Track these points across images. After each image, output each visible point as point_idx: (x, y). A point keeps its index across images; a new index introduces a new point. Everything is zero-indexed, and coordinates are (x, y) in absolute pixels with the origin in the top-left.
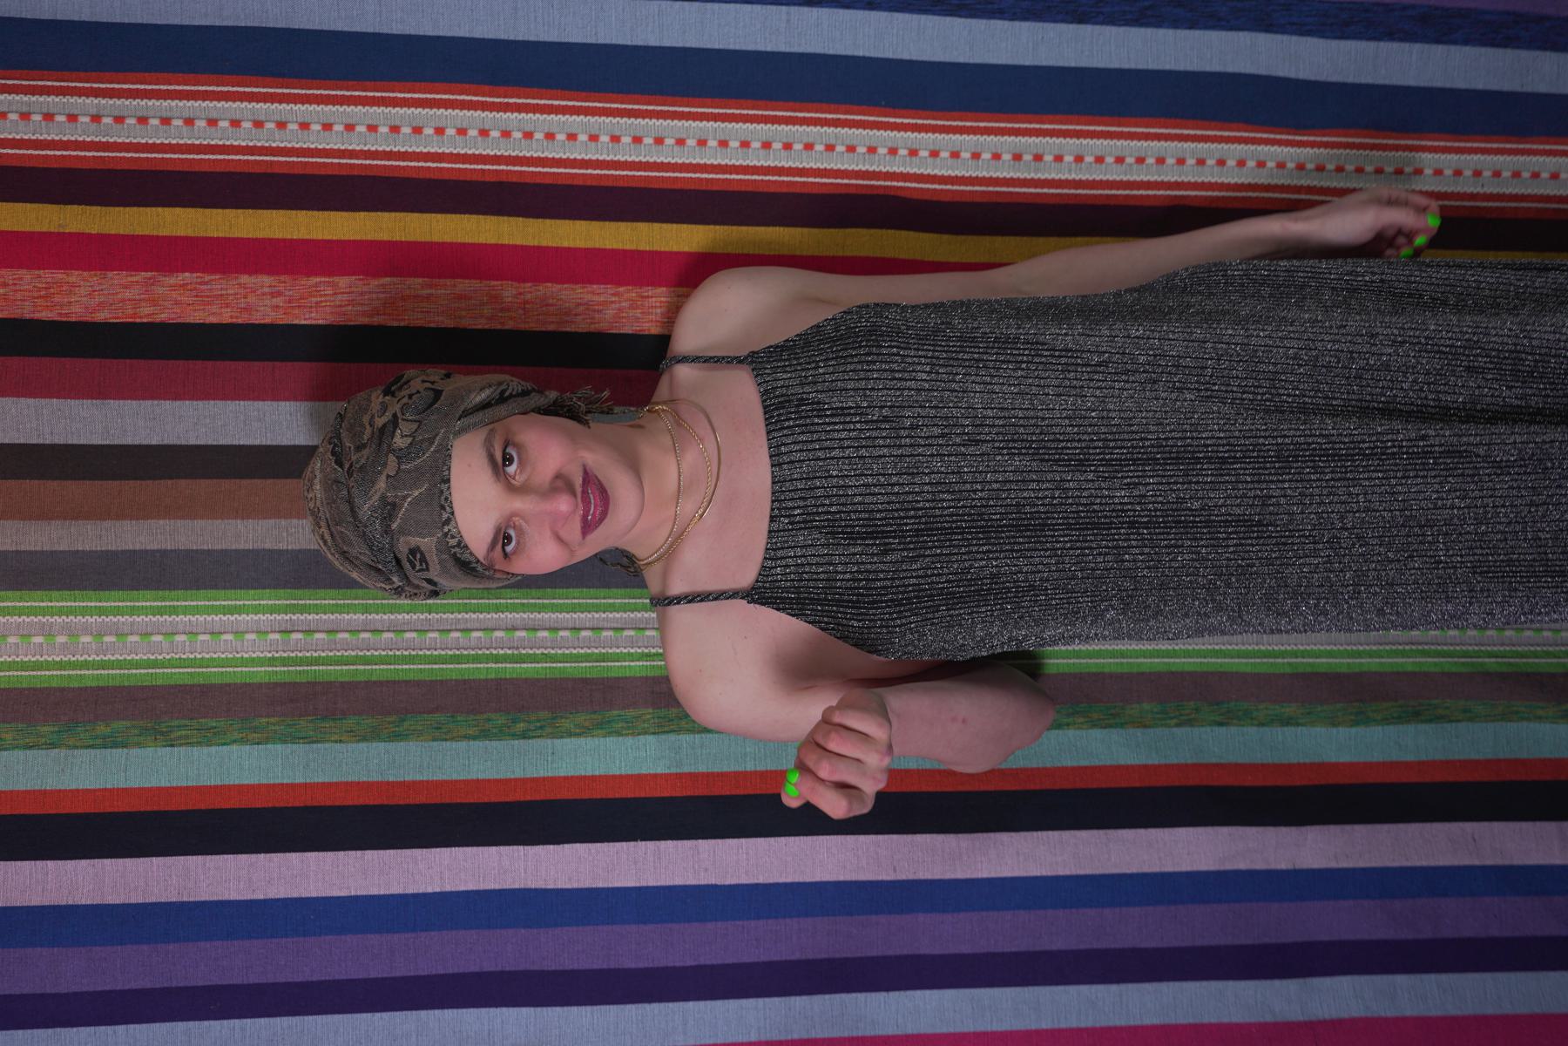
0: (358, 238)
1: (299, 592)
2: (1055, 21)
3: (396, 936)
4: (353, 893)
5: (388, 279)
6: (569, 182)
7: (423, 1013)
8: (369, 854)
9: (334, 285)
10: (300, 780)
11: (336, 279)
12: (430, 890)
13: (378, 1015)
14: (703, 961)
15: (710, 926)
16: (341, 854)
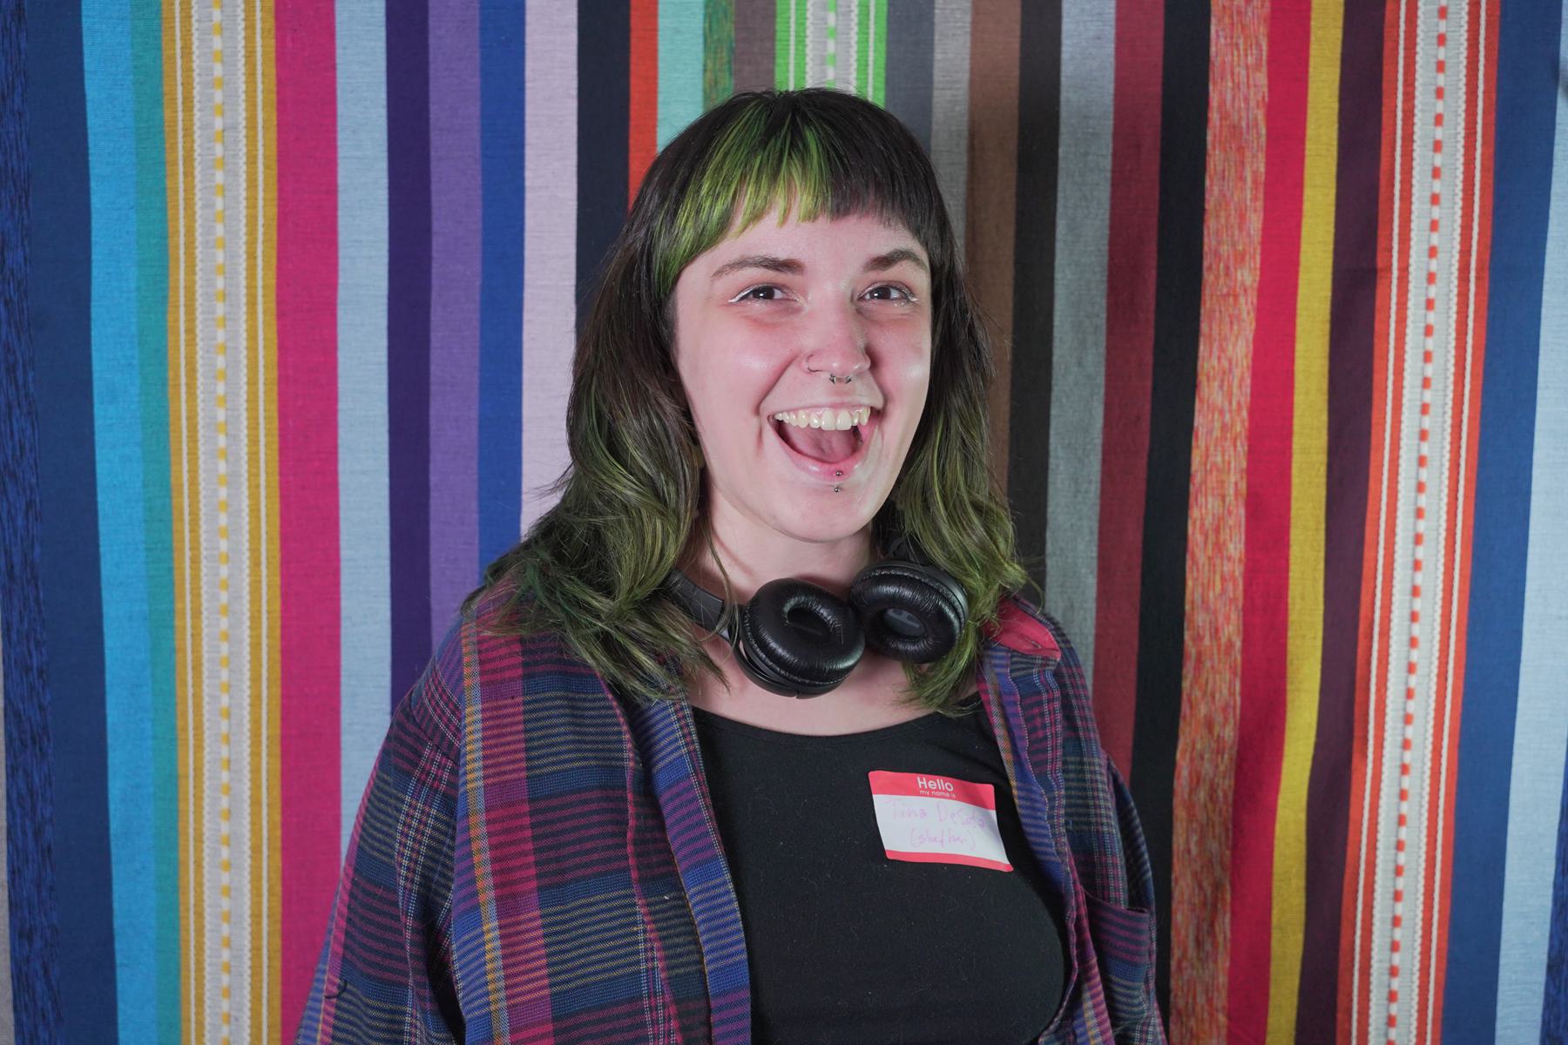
0: (1311, 97)
1: (883, 23)
2: (1552, 937)
3: (476, 135)
4: (528, 85)
5: (1263, 131)
6: (1377, 352)
7: (383, 165)
8: (572, 105)
9: (1258, 67)
10: (663, 23)
11: (1264, 69)
12: (528, 174)
13: (383, 112)
14: (433, 494)
15: (474, 505)
16: (574, 72)
